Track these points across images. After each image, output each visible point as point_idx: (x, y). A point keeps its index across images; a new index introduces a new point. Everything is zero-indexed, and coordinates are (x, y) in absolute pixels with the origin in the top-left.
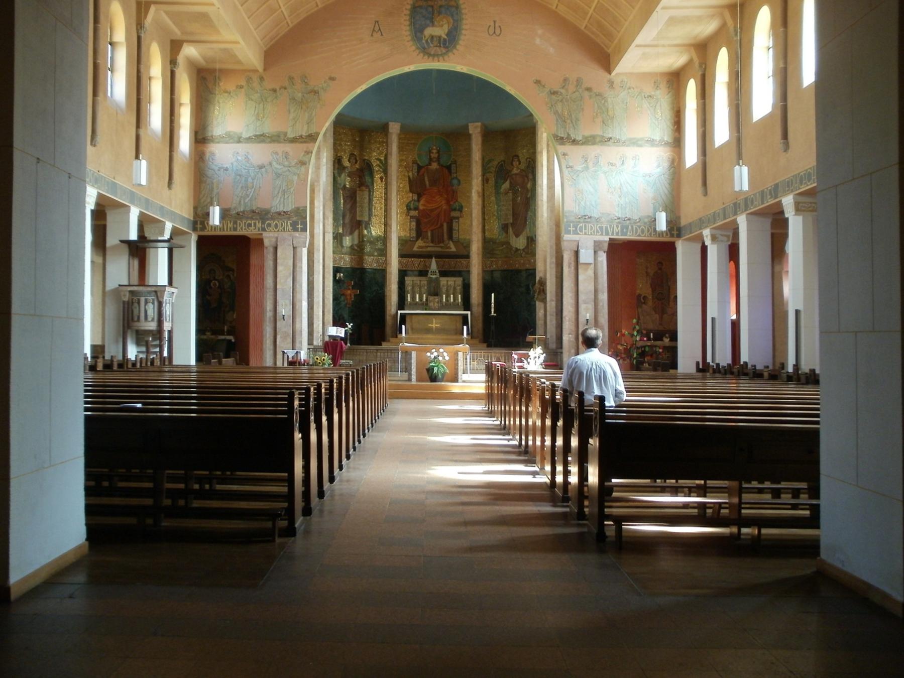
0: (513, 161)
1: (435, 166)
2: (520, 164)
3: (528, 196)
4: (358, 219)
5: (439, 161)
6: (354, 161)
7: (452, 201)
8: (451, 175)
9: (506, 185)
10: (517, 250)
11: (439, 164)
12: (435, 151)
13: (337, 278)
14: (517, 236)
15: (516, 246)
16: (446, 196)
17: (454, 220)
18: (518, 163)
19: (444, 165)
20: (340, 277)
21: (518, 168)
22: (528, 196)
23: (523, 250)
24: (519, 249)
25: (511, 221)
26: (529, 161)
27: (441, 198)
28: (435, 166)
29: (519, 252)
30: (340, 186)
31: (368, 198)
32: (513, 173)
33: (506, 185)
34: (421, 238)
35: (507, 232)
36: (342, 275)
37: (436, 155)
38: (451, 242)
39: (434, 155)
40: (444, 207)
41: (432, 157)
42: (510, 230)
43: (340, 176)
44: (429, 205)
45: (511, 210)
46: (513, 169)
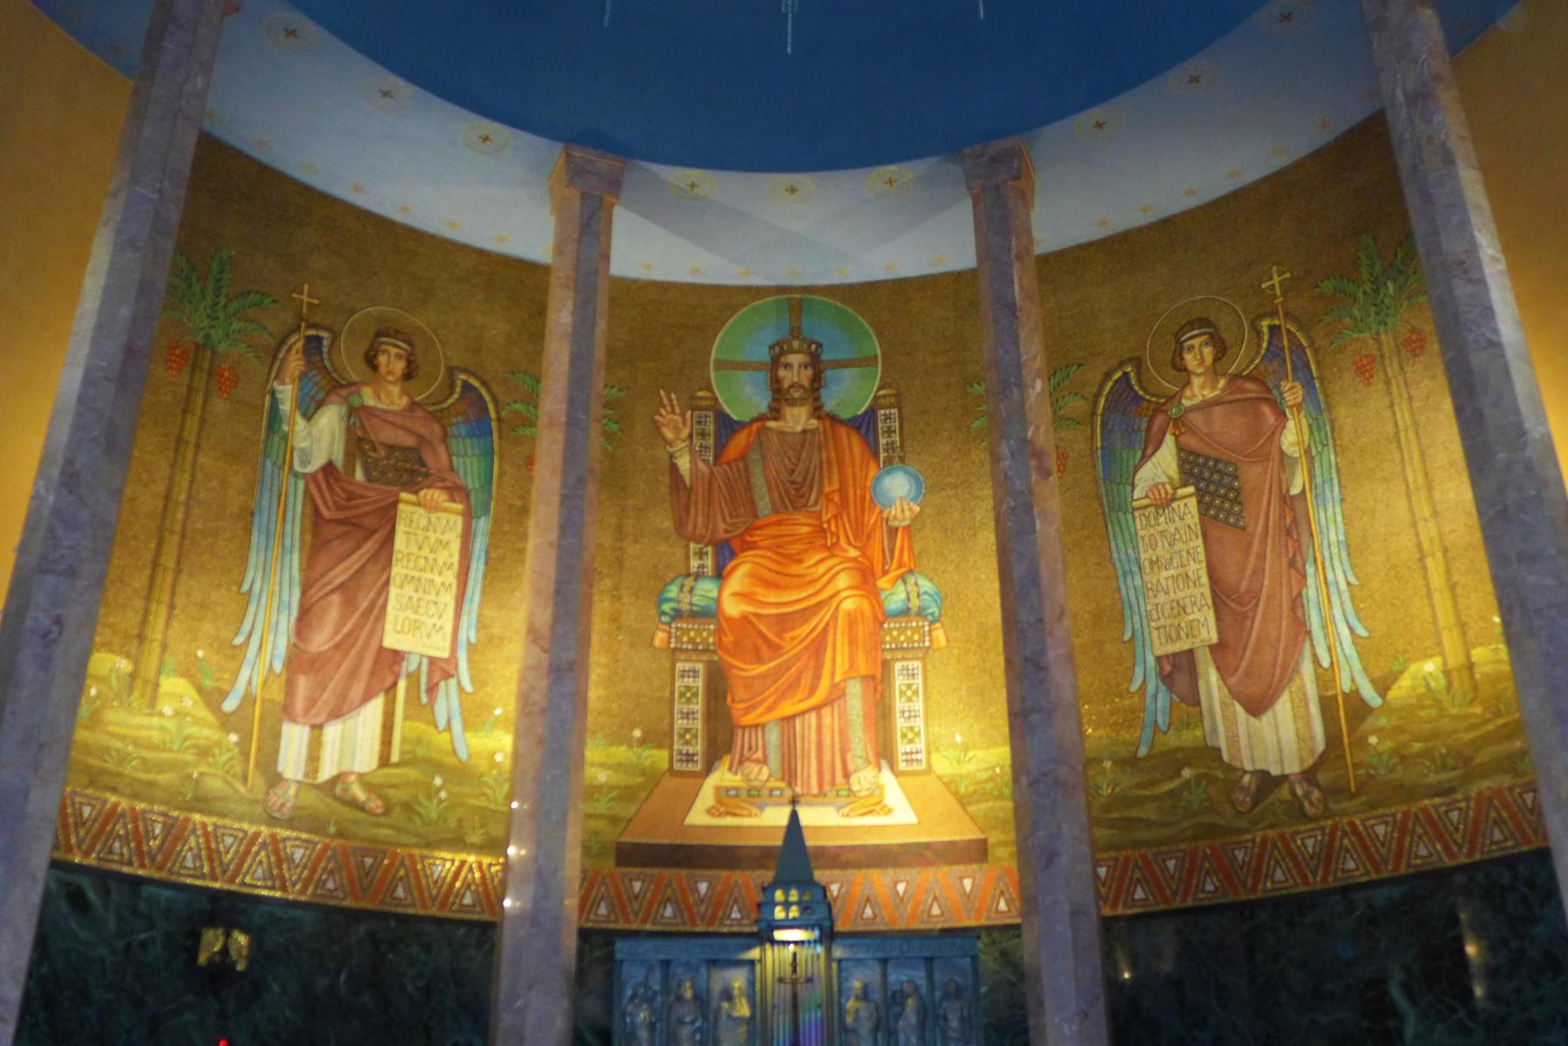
0: (1179, 351)
1: (798, 418)
2: (1216, 360)
3: (1295, 490)
4: (391, 641)
5: (817, 399)
6: (399, 367)
7: (885, 573)
8: (876, 455)
9: (1164, 463)
10: (1268, 783)
11: (817, 411)
12: (795, 359)
13: (203, 959)
14: (1257, 707)
15: (1260, 766)
16: (853, 553)
17: (898, 666)
18: (1208, 352)
19: (846, 415)
20: (225, 950)
21: (1215, 371)
22: (1295, 490)
23: (1309, 775)
24: (1284, 778)
25: (1214, 638)
26: (1272, 328)
27: (829, 563)
28: (798, 418)
29: (1284, 792)
30: (305, 463)
31: (456, 546)
32: (1186, 403)
33: (1164, 463)
34: (727, 760)
35: (1193, 698)
36: (241, 939)
37: (805, 376)
38: (886, 776)
39: (795, 372)
40: (849, 605)
41: (786, 384)
42: (1211, 680)
43: (308, 417)
44: (772, 597)
45: (1205, 580)
46: (1188, 383)
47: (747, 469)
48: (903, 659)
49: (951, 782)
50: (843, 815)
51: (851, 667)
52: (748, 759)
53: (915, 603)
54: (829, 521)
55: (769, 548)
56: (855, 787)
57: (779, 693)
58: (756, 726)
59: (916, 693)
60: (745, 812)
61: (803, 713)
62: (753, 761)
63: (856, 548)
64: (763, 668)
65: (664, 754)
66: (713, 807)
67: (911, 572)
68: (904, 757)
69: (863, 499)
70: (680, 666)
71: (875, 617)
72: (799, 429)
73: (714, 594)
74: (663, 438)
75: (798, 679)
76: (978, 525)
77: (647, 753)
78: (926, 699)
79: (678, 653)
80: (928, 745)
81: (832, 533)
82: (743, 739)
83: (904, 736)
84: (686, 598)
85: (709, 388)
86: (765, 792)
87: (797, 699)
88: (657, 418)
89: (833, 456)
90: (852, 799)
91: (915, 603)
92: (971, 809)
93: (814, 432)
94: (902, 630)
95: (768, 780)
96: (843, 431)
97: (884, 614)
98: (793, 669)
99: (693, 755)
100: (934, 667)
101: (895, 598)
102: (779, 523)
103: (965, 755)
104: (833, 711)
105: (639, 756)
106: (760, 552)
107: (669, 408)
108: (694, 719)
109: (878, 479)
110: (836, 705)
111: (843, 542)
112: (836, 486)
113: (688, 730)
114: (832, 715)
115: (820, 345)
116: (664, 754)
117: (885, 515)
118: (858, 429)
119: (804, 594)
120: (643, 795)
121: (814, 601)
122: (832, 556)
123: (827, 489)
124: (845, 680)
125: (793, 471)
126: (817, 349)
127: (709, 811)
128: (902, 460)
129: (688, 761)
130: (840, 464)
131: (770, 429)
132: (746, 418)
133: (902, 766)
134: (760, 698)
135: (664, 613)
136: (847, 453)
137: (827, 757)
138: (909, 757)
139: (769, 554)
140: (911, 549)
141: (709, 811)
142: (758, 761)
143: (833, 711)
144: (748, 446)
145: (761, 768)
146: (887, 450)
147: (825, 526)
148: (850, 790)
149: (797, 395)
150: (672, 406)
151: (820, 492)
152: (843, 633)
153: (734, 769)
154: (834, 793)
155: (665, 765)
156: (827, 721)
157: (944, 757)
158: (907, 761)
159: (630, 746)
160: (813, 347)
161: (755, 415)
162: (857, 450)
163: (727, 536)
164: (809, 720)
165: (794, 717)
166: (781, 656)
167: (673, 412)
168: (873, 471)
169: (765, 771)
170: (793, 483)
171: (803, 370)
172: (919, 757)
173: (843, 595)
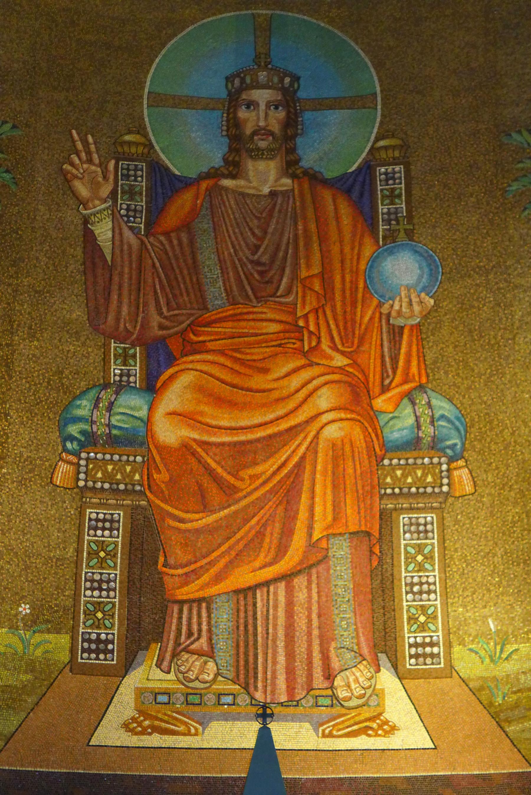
5: (292, 150)
7: (384, 389)
16: (340, 361)
17: (404, 519)
27: (305, 375)
34: (155, 648)
47: (192, 242)
48: (411, 509)
49: (481, 689)
50: (324, 736)
51: (335, 519)
52: (186, 650)
53: (427, 431)
54: (306, 317)
55: (222, 353)
56: (342, 694)
57: (233, 553)
58: (199, 601)
59: (429, 558)
60: (182, 728)
61: (267, 584)
62: (193, 653)
63: (343, 353)
64: (211, 519)
65: (64, 640)
66: (134, 719)
67: (421, 388)
68: (413, 651)
69: (354, 289)
70: (90, 513)
71: (370, 449)
72: (266, 190)
73: (143, 413)
74: (75, 194)
75: (260, 535)
76: (517, 324)
77: (38, 638)
78: (444, 568)
79: (89, 495)
80: (448, 633)
81: (311, 333)
82: (180, 618)
83: (412, 619)
84: (103, 419)
85: (141, 130)
86: (211, 699)
87: (257, 564)
88: (67, 167)
89: (313, 226)
90: (337, 710)
91: (427, 431)
92: (511, 729)
93: (285, 194)
94: (408, 469)
95: (214, 680)
96: (327, 195)
97: (383, 446)
98: (254, 521)
99: (107, 642)
100: (457, 522)
101: (399, 424)
102: (235, 318)
103: (502, 651)
104: (309, 582)
105: (26, 644)
106: (209, 357)
107: (83, 155)
108: (108, 590)
109: (374, 261)
110: (314, 571)
111: (325, 345)
112: (316, 270)
113: (98, 606)
114: (309, 588)
115: (296, 79)
116: (64, 640)
117: (385, 310)
118: (348, 192)
119: (270, 416)
120: (31, 700)
121: (284, 425)
122: (311, 365)
123: (304, 273)
124: (328, 537)
125: (258, 247)
126: (291, 84)
127: (126, 726)
128: (410, 234)
129: (97, 651)
130: (323, 239)
131: (226, 189)
132: (193, 174)
133: (410, 664)
134: (204, 562)
135: (72, 438)
136: (333, 224)
137: (301, 649)
138: (420, 650)
139: (222, 360)
140: (421, 357)
141: (126, 726)
142: (200, 653)
143: (309, 582)
144: (194, 213)
145: (205, 663)
146: (388, 222)
147: (301, 323)
148: (334, 696)
149: (263, 144)
150: (89, 153)
151: (294, 276)
152: (324, 473)
153: (165, 664)
154: (311, 701)
155: (65, 657)
156: (301, 596)
157: (471, 650)
158: (417, 656)
159: (13, 628)
160: (287, 80)
161: (205, 170)
162: (346, 221)
163: (161, 333)
164: (276, 594)
165: (253, 589)
166: (237, 501)
167: (90, 161)
168: (368, 250)
169: (211, 665)
170: (258, 263)
171: (272, 112)
172: (435, 650)
173: (325, 418)
